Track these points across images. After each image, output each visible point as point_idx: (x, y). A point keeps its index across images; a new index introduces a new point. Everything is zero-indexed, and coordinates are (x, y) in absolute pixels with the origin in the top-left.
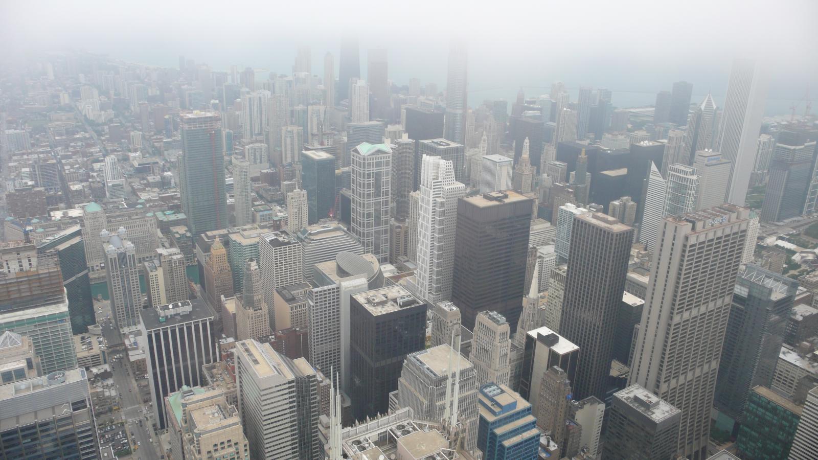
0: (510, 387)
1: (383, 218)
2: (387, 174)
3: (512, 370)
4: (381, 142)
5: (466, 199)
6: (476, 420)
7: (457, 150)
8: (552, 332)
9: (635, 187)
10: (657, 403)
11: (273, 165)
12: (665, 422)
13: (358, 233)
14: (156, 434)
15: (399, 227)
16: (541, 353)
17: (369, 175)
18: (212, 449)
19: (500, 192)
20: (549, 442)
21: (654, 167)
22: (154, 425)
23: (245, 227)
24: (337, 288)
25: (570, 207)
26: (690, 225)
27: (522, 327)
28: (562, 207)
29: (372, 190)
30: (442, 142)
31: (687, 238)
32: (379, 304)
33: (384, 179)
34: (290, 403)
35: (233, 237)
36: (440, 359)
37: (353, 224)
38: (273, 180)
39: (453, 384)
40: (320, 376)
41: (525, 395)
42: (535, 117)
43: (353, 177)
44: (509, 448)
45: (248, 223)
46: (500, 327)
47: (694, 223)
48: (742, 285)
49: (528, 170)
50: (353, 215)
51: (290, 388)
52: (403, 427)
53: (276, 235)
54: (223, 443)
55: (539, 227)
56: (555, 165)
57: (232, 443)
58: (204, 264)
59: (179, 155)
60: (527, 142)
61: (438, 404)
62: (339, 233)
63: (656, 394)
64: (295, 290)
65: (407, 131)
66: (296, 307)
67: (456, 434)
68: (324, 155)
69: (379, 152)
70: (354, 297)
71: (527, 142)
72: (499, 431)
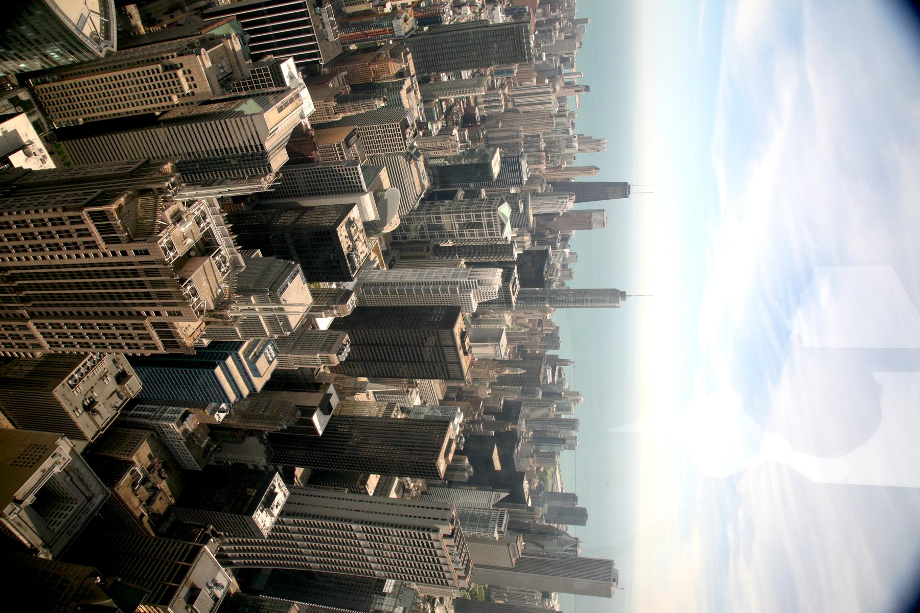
0: (275, 370)
1: (436, 233)
2: (481, 235)
3: (293, 371)
4: (513, 226)
5: (461, 314)
6: (238, 338)
7: (509, 302)
8: (334, 407)
9: (484, 478)
10: (272, 515)
11: (483, 118)
12: (254, 524)
13: (419, 209)
14: (196, 9)
15: (428, 250)
16: (314, 399)
17: (478, 216)
18: (186, 68)
19: (470, 347)
20: (223, 412)
21: (504, 495)
22: (206, 7)
23: (418, 92)
24: (363, 190)
25: (459, 419)
26: (450, 533)
27: (336, 378)
28: (459, 410)
29: (464, 220)
30: (516, 288)
31: (436, 531)
32: (349, 232)
33: (476, 231)
34: (241, 148)
35: (408, 82)
36: (297, 294)
37: (428, 203)
38: (468, 120)
39: (271, 310)
40: (271, 178)
41: (268, 386)
42: (546, 377)
43: (476, 201)
44: (214, 374)
45: (423, 96)
46: (335, 356)
47: (451, 536)
48: (395, 586)
49: (494, 374)
50: (437, 203)
51: (256, 146)
52: (225, 262)
53: (413, 125)
54: (192, 79)
55: (436, 388)
56: (500, 400)
57: (194, 90)
58: (378, 52)
59: (488, 21)
60: (520, 372)
61: (252, 298)
62: (418, 189)
63: (281, 514)
64: (358, 147)
65: (525, 252)
66: (340, 150)
67: (221, 316)
68: (496, 168)
69: (503, 225)
70: (355, 208)
71: (520, 372)
72: (230, 361)
